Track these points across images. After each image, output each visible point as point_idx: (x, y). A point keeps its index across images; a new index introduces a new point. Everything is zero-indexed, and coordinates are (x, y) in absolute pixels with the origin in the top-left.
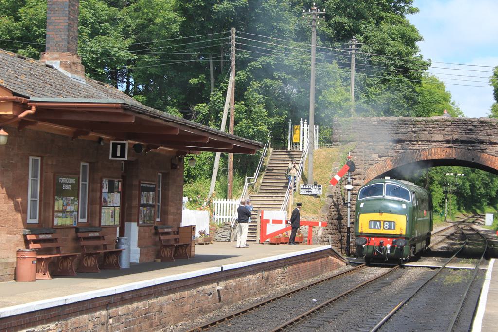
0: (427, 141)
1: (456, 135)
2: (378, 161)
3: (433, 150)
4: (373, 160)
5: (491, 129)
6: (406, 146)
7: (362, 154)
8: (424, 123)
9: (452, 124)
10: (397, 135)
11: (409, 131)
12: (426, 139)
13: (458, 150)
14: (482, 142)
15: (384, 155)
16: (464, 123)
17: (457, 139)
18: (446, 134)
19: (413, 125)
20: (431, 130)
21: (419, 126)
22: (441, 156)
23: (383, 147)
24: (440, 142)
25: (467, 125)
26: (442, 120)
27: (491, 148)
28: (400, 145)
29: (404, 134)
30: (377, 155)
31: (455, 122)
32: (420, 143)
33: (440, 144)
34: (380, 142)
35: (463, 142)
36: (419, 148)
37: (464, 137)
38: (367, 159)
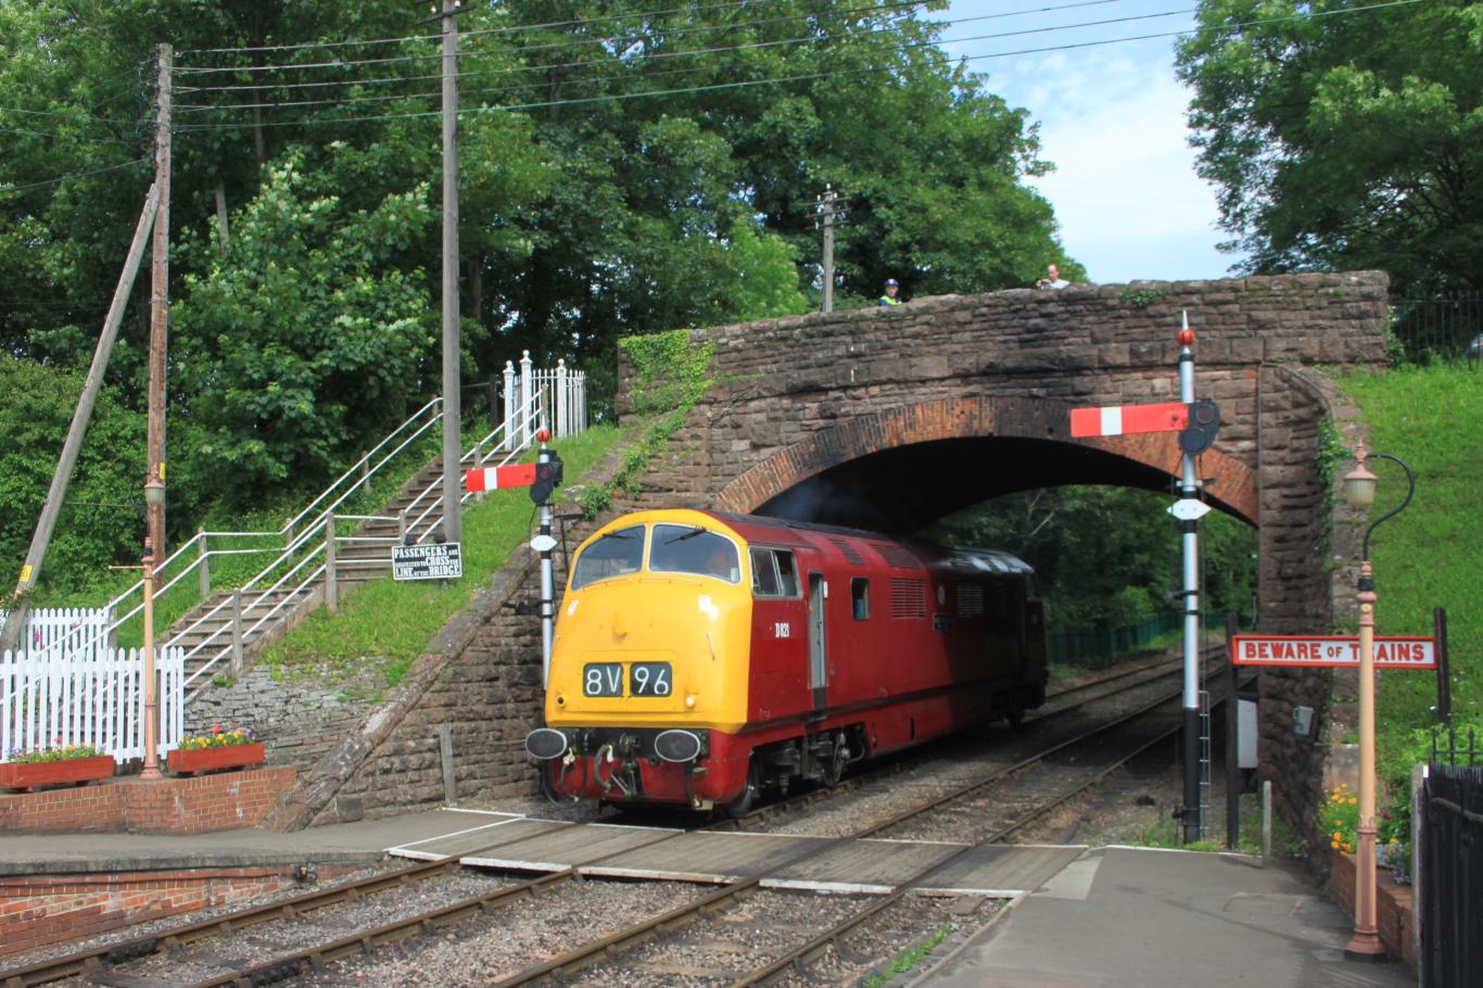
0: (898, 382)
1: (990, 354)
2: (751, 461)
3: (919, 411)
4: (736, 462)
5: (1105, 318)
6: (833, 404)
7: (698, 443)
8: (887, 326)
9: (975, 316)
10: (803, 372)
11: (840, 357)
12: (893, 376)
13: (1001, 404)
14: (1077, 369)
15: (767, 442)
16: (1012, 308)
17: (991, 365)
18: (955, 353)
19: (851, 333)
20: (907, 346)
21: (871, 336)
22: (943, 427)
23: (762, 417)
24: (942, 379)
25: (1022, 314)
26: (939, 309)
27: (1108, 384)
28: (815, 405)
29: (826, 365)
30: (744, 445)
31: (984, 310)
32: (875, 390)
33: (941, 389)
34: (752, 399)
35: (1011, 373)
36: (871, 408)
37: (1015, 358)
38: (717, 456)
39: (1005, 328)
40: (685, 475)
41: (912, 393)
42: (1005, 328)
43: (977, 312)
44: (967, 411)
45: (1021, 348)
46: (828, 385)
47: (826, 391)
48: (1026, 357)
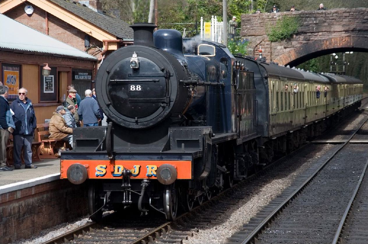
6: (309, 37)
11: (311, 24)
15: (289, 47)
19: (314, 17)
28: (303, 37)
29: (307, 26)
32: (320, 33)
36: (320, 39)
39: (359, 18)
40: (265, 55)
41: (331, 35)
42: (359, 18)
43: (350, 13)
44: (347, 40)
45: (362, 24)
46: (308, 32)
47: (306, 33)
48: (364, 27)
